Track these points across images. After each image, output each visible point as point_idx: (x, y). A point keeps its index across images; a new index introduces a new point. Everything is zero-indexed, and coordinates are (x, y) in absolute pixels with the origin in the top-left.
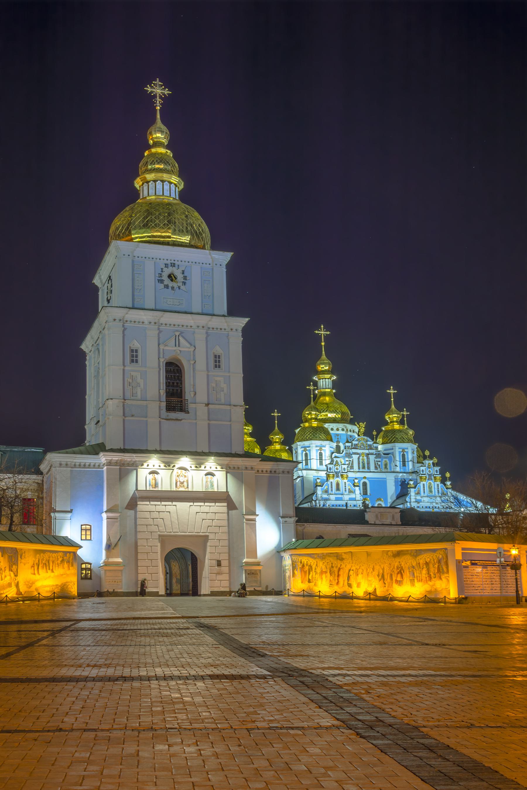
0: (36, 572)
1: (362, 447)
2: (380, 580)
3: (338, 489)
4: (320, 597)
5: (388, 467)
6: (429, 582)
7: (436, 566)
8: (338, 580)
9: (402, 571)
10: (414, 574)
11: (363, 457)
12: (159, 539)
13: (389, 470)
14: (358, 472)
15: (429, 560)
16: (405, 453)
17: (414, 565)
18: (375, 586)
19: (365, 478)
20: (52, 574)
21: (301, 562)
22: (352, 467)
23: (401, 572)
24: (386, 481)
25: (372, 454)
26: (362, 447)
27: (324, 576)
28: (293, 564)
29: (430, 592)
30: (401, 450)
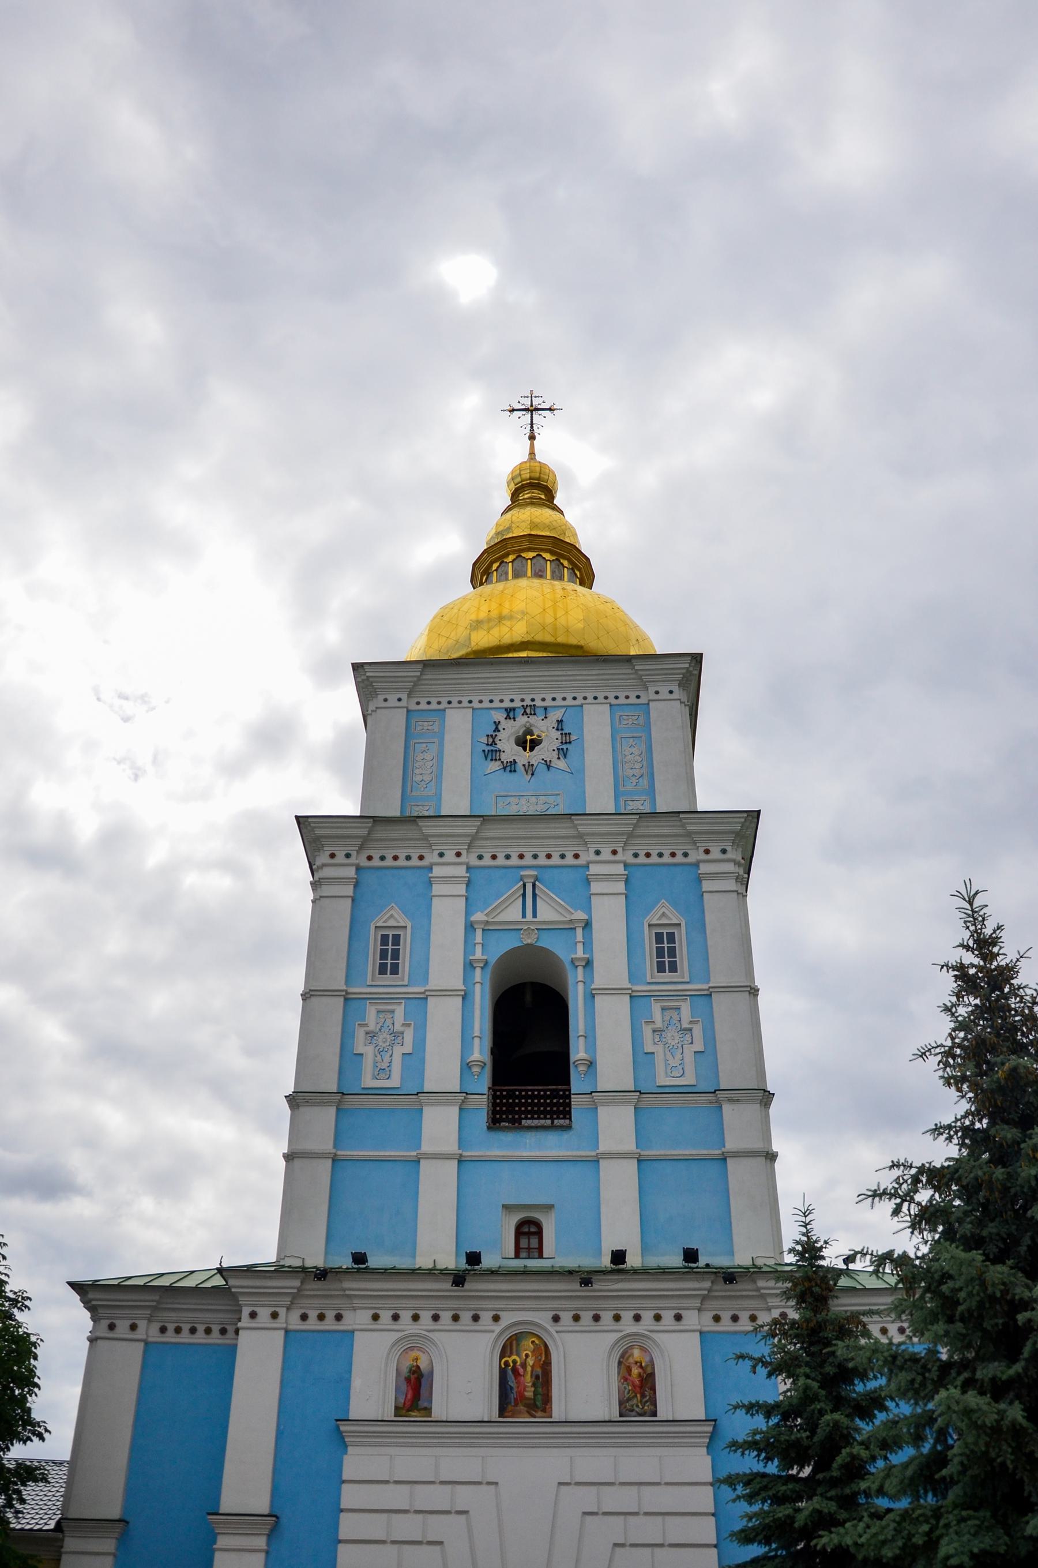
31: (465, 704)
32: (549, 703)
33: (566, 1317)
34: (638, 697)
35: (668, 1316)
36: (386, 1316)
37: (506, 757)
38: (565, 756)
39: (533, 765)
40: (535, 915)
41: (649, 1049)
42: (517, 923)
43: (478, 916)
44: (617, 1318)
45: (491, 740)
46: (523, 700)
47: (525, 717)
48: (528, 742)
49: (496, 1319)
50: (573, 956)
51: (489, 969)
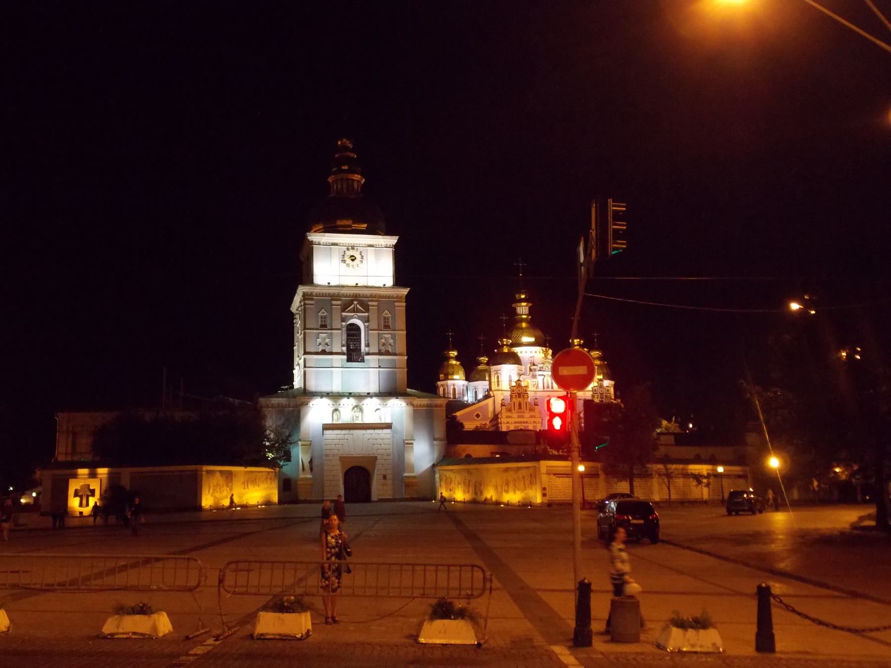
0: (246, 487)
2: (495, 489)
3: (520, 407)
4: (454, 501)
7: (529, 479)
10: (515, 485)
12: (340, 460)
14: (543, 391)
17: (516, 478)
20: (259, 488)
21: (445, 476)
22: (537, 387)
23: (507, 484)
26: (547, 369)
27: (460, 486)
29: (524, 498)
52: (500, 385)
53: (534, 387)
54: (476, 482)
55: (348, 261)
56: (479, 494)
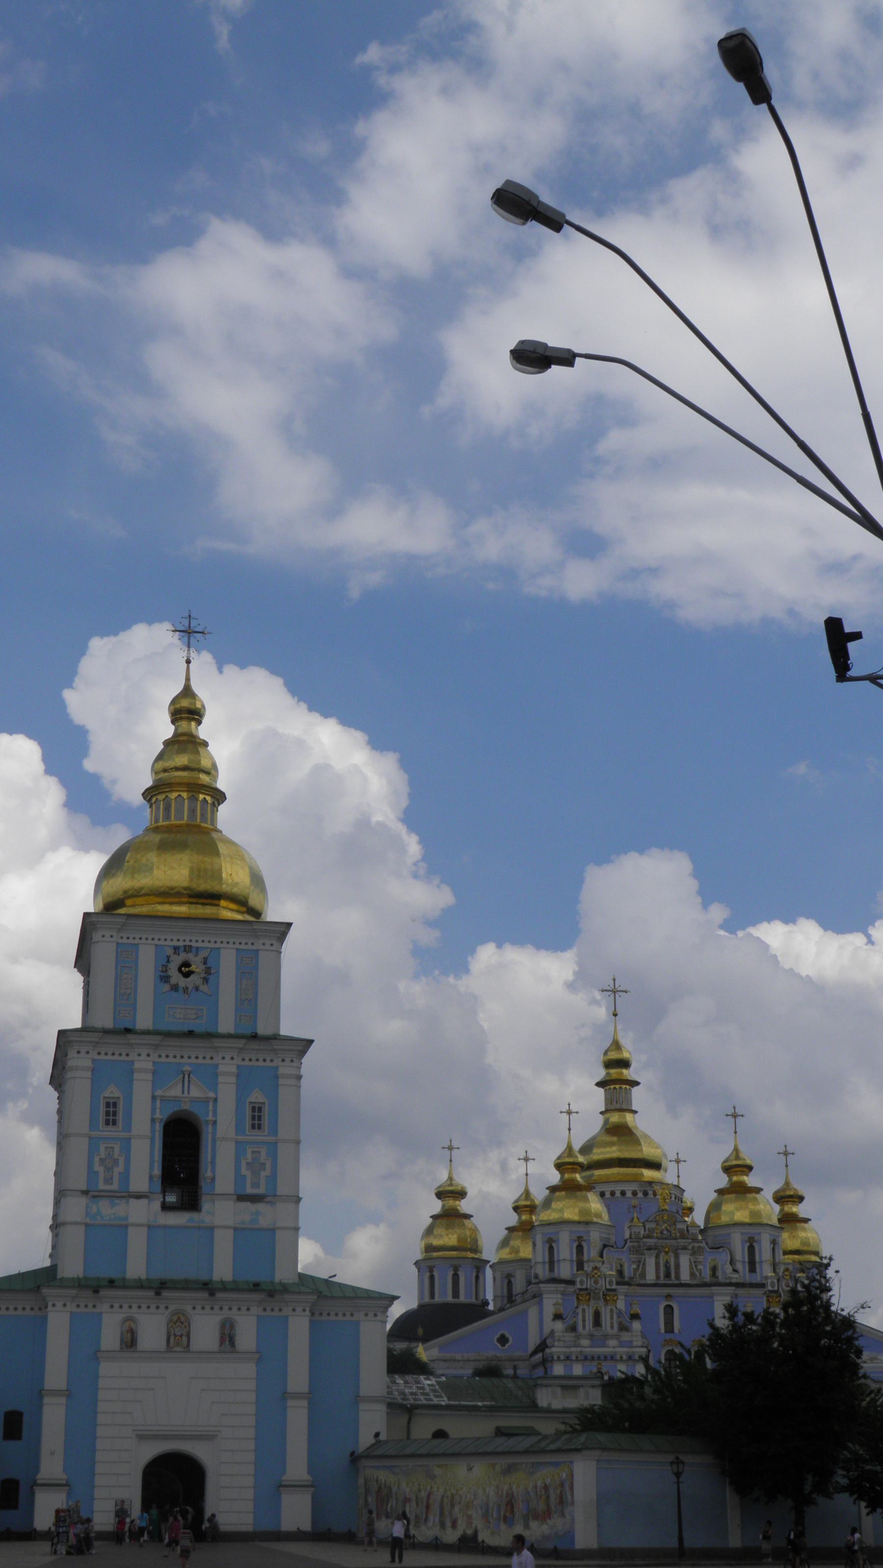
1: (665, 1232)
3: (597, 1322)
5: (719, 1274)
6: (548, 1521)
7: (558, 1492)
8: (427, 1514)
9: (513, 1500)
11: (667, 1253)
13: (721, 1279)
15: (549, 1480)
16: (755, 1245)
18: (476, 1527)
19: (669, 1297)
21: (377, 1481)
22: (643, 1275)
24: (713, 1302)
25: (685, 1248)
26: (665, 1232)
28: (366, 1484)
30: (746, 1238)
31: (150, 941)
32: (200, 944)
33: (199, 1307)
34: (253, 944)
35: (244, 1308)
36: (116, 1305)
37: (173, 981)
38: (207, 982)
39: (187, 988)
40: (189, 1093)
41: (244, 1171)
42: (179, 1097)
43: (159, 1093)
44: (221, 1309)
45: (164, 969)
46: (184, 941)
47: (184, 954)
48: (185, 969)
49: (167, 1308)
50: (208, 1119)
51: (163, 1124)
52: (556, 1270)
53: (635, 1274)
54: (443, 1497)
55: (176, 977)
56: (448, 1524)
